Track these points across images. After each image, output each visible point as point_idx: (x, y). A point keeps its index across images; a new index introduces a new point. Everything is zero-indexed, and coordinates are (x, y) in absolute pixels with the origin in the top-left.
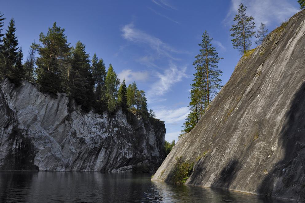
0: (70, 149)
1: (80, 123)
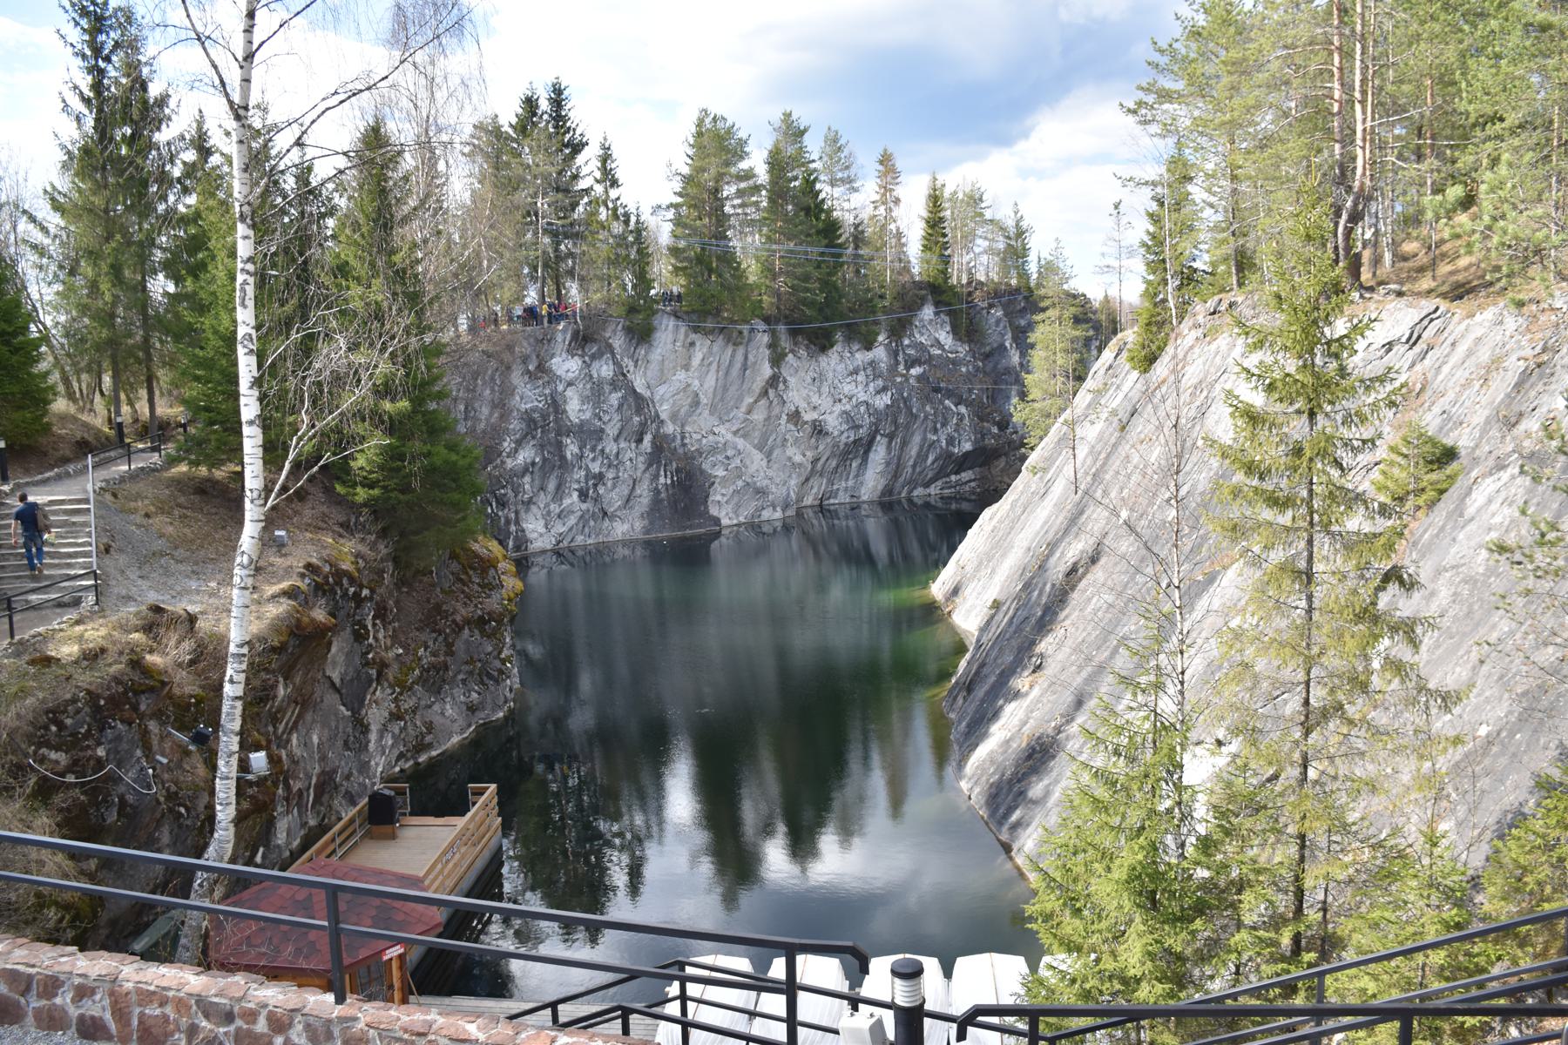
0: (790, 459)
1: (809, 380)
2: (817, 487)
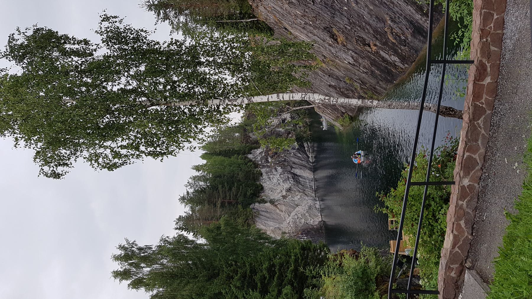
2: (309, 191)
